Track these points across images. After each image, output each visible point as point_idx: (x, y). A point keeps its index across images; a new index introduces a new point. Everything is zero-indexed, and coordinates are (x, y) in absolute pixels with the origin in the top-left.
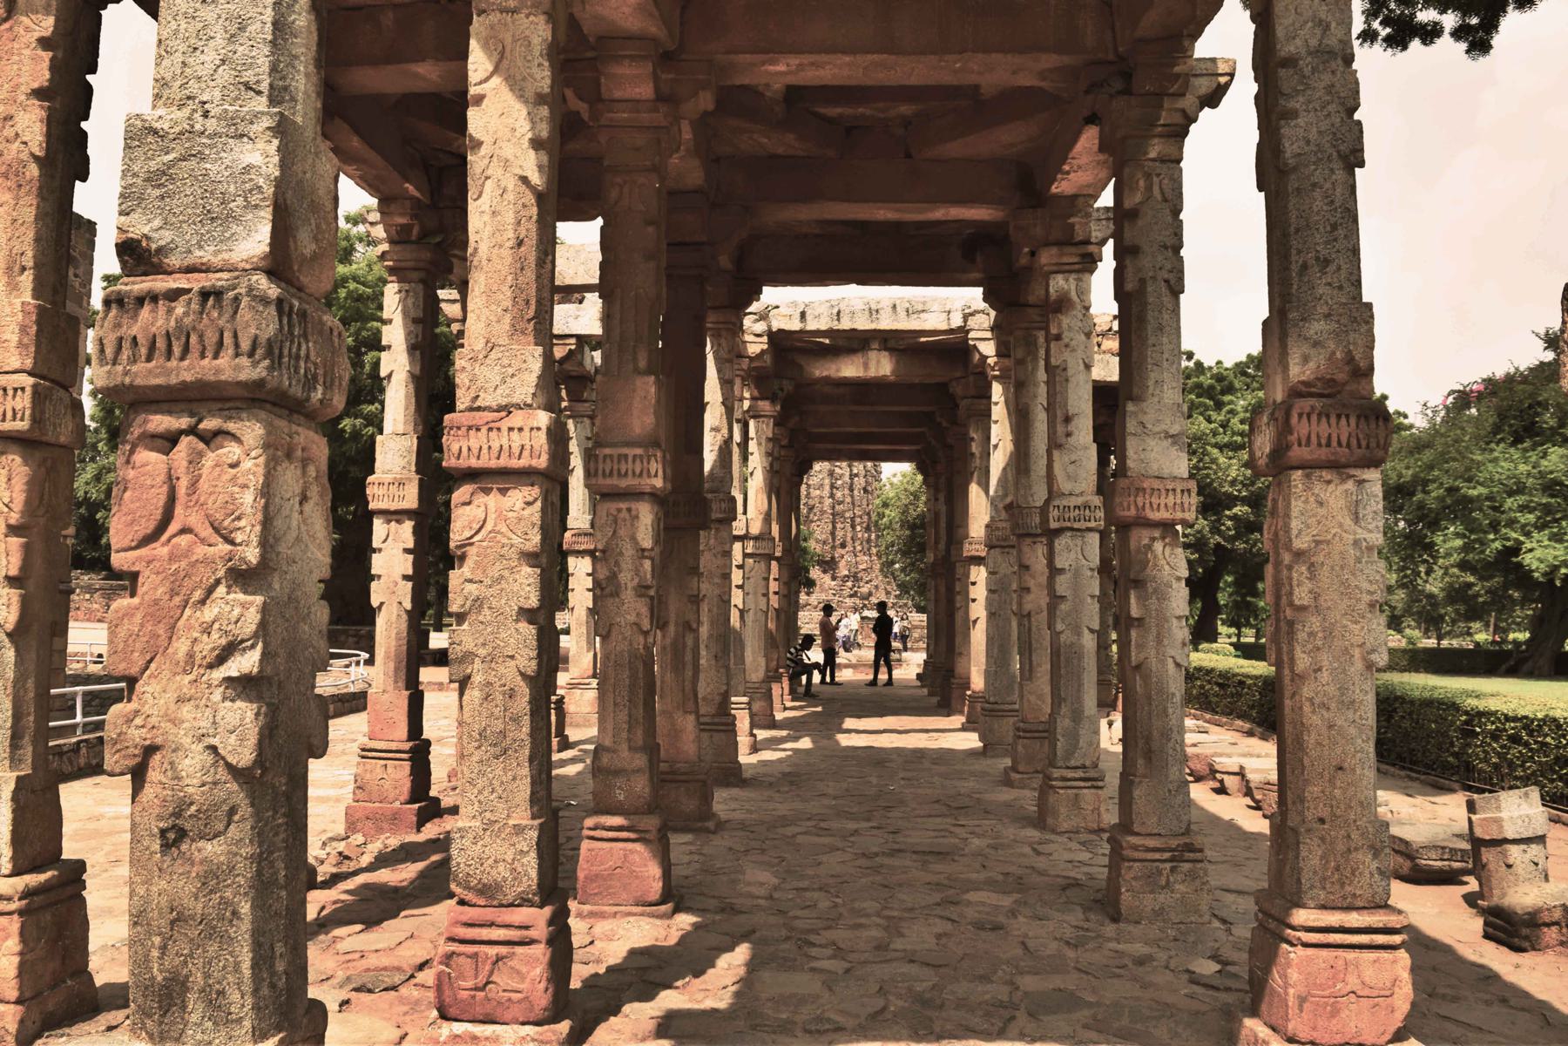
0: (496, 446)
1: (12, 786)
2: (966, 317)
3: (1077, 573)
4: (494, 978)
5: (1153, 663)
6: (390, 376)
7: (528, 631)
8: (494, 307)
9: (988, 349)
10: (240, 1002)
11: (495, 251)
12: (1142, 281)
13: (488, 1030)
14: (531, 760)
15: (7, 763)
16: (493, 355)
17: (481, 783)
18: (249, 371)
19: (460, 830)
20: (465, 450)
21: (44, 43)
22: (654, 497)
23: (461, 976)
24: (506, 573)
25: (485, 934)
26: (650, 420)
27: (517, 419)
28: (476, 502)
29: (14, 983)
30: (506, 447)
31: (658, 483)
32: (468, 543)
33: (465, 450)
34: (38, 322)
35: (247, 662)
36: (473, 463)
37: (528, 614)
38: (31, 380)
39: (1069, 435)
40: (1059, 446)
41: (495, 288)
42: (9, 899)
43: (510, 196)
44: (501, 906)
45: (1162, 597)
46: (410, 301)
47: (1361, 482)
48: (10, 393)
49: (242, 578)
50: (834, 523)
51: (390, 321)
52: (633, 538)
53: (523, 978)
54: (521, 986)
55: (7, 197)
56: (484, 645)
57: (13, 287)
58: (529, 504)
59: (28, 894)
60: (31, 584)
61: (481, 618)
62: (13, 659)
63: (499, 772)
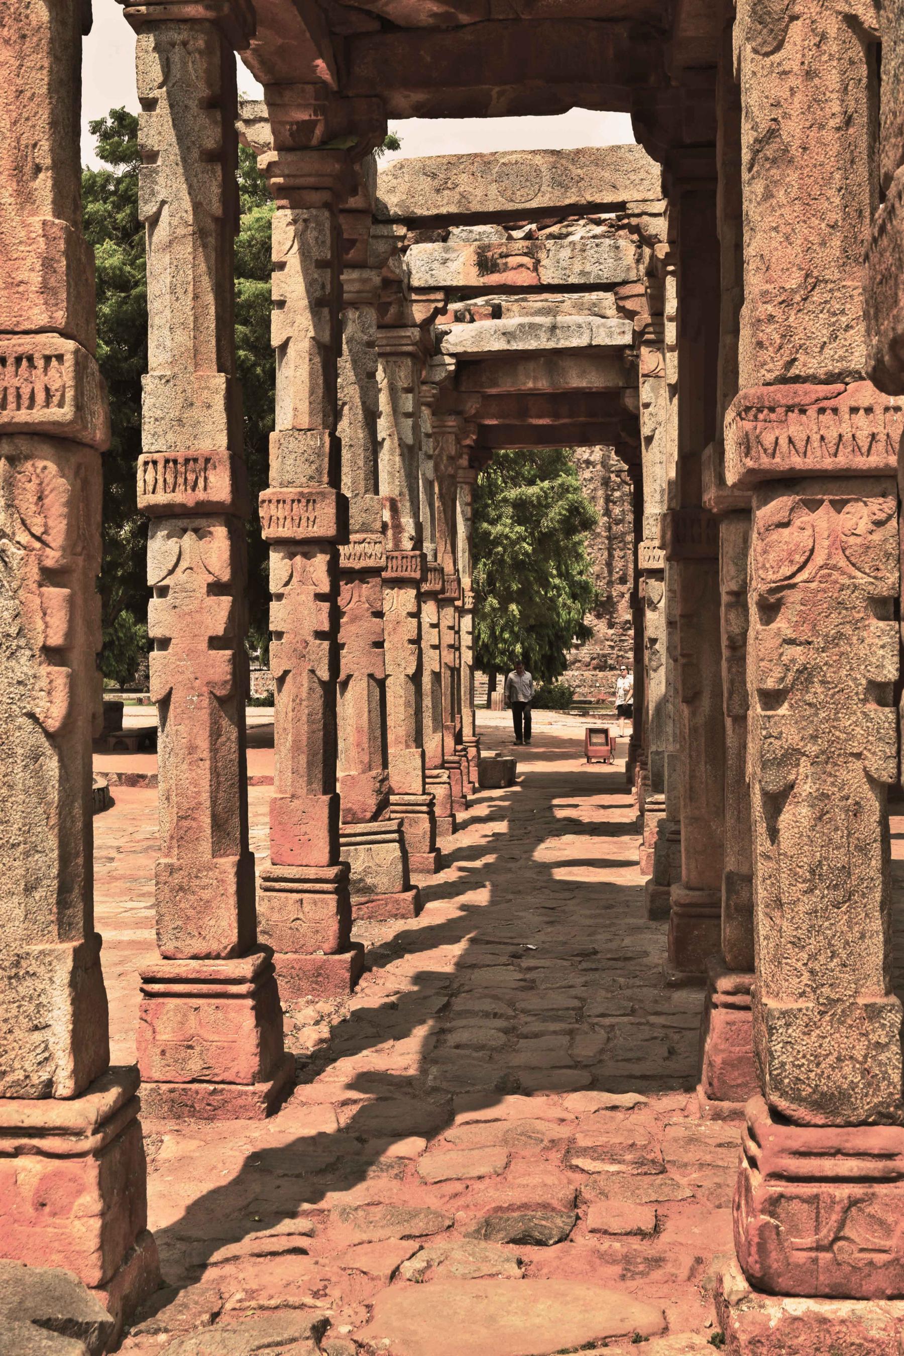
0: (832, 435)
1: (69, 964)
4: (847, 1232)
6: (284, 346)
8: (815, 222)
11: (813, 134)
13: (844, 1308)
14: (882, 910)
15: (54, 928)
16: (816, 297)
17: (813, 944)
19: (784, 1014)
20: (783, 442)
23: (795, 1230)
24: (848, 630)
25: (829, 1166)
28: (797, 523)
29: (95, 1259)
30: (847, 437)
32: (786, 584)
33: (783, 442)
34: (67, 254)
36: (797, 462)
38: (68, 346)
41: (816, 192)
42: (78, 1133)
43: (833, 47)
44: (849, 1124)
46: (311, 235)
48: (40, 363)
50: (610, 550)
51: (282, 266)
53: (887, 1229)
54: (886, 1244)
55: (4, 54)
56: (814, 738)
57: (25, 198)
58: (879, 524)
59: (101, 1125)
60: (76, 656)
61: (809, 697)
62: (56, 773)
63: (842, 926)
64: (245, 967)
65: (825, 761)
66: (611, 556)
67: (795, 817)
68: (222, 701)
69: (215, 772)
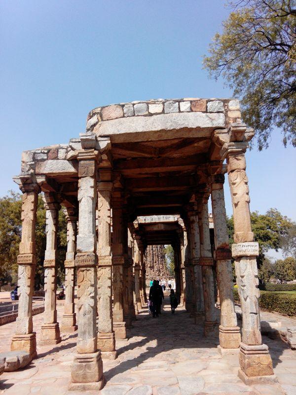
2: (178, 219)
3: (199, 273)
5: (208, 290)
7: (110, 289)
9: (183, 225)
10: (92, 333)
12: (202, 224)
13: (105, 353)
18: (93, 263)
21: (32, 202)
22: (123, 265)
26: (122, 251)
27: (107, 258)
29: (29, 352)
31: (123, 262)
35: (93, 295)
37: (109, 287)
39: (196, 246)
40: (194, 249)
45: (209, 278)
47: (228, 262)
49: (92, 286)
52: (119, 272)
57: (29, 240)
64: (54, 325)
65: (103, 294)
66: (153, 258)
67: (101, 300)
68: (53, 290)
69: (52, 300)
